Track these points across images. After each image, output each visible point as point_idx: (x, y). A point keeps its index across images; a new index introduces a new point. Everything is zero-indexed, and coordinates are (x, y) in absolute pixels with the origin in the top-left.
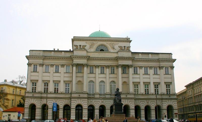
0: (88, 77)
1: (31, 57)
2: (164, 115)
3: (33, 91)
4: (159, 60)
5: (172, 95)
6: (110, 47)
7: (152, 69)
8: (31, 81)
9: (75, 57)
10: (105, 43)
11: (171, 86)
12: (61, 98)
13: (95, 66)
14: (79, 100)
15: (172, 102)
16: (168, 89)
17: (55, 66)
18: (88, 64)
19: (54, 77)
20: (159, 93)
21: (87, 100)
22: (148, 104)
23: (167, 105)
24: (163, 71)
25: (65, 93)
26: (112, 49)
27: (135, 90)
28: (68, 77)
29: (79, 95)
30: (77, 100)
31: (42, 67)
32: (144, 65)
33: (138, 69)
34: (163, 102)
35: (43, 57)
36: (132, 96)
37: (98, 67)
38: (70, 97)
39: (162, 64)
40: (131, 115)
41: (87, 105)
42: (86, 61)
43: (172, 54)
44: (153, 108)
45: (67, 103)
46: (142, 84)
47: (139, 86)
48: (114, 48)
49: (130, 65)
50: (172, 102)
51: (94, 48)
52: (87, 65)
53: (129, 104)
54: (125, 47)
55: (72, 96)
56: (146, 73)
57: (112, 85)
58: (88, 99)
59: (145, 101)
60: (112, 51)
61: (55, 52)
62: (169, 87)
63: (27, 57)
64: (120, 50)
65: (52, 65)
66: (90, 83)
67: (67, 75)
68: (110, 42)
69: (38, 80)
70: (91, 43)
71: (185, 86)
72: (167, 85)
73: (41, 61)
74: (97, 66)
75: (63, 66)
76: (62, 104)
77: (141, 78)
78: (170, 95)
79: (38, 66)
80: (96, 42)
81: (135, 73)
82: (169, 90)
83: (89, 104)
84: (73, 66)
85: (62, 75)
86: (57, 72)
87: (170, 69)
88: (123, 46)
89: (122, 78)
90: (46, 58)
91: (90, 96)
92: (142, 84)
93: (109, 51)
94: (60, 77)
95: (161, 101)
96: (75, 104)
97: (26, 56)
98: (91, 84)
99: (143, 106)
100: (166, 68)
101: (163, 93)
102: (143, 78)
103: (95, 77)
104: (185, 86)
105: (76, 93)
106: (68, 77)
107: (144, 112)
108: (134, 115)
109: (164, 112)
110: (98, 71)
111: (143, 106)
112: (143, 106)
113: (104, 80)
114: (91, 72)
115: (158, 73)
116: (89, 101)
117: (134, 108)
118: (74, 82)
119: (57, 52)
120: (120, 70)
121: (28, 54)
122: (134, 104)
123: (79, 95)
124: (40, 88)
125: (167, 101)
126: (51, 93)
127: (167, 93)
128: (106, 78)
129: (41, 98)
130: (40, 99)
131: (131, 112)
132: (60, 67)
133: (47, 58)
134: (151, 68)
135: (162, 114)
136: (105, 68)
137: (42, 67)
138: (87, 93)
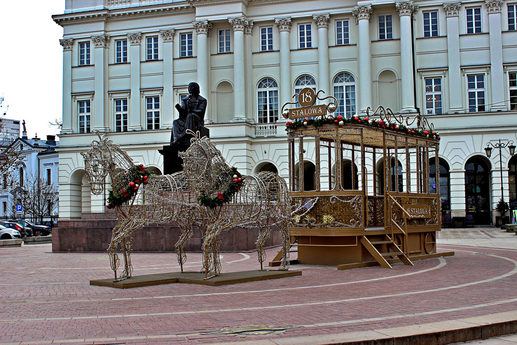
8: (74, 95)
13: (277, 21)
17: (144, 42)
18: (250, 19)
21: (244, 146)
31: (105, 47)
33: (441, 16)
35: (102, 13)
37: (290, 25)
42: (239, 7)
52: (248, 27)
63: (59, 20)
65: (136, 38)
66: (265, 87)
75: (169, 35)
77: (453, 50)
86: (153, 57)
97: (53, 16)
98: (268, 89)
103: (279, 65)
111: (457, 159)
114: (267, 48)
121: (61, 10)
124: (100, 116)
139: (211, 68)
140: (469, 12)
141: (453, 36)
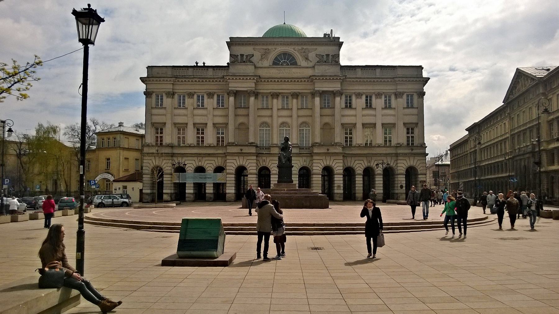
0: (259, 116)
1: (149, 81)
2: (399, 185)
3: (157, 144)
4: (396, 79)
5: (417, 146)
6: (301, 55)
7: (381, 98)
9: (233, 79)
10: (289, 49)
11: (416, 131)
12: (209, 155)
14: (241, 158)
15: (415, 161)
16: (410, 135)
19: (195, 117)
20: (394, 143)
22: (369, 164)
23: (405, 167)
24: (402, 101)
25: (216, 145)
26: (304, 61)
27: (346, 138)
28: (221, 116)
29: (241, 150)
30: (237, 158)
31: (173, 98)
32: (364, 91)
33: (354, 98)
34: (399, 161)
35: (172, 79)
36: (339, 150)
38: (224, 153)
39: (401, 88)
40: (336, 185)
41: (255, 168)
42: (253, 85)
43: (423, 68)
44: (379, 172)
45: (220, 164)
46: (359, 126)
47: (354, 132)
48: (307, 59)
49: (337, 91)
50: (415, 161)
51: (269, 58)
52: (256, 95)
53: (333, 165)
54: (328, 55)
55: (228, 151)
56: (369, 105)
57: (303, 130)
58: (257, 156)
59: (365, 159)
60: (303, 63)
61: (198, 68)
62: (412, 133)
63: (143, 80)
64: (318, 62)
65: (191, 95)
67: (217, 112)
68: (300, 48)
69: (165, 124)
70: (263, 49)
71: (467, 130)
72: (408, 129)
73: (169, 87)
74: (275, 95)
76: (211, 165)
78: (413, 148)
79: (165, 97)
80: (273, 47)
81: (349, 105)
82: (412, 137)
83: (259, 165)
84: (229, 94)
85: (210, 114)
87: (415, 97)
88: (324, 54)
89: (321, 116)
90: (178, 81)
91: (261, 151)
92: (359, 126)
93: (299, 64)
94: (206, 116)
95: (395, 158)
96: (234, 166)
97: (141, 78)
98: (265, 128)
99: (359, 167)
100: (408, 96)
101: (398, 144)
102: (363, 116)
103: (271, 116)
104: (467, 130)
105: (236, 145)
106: (221, 116)
107: (362, 179)
108: (342, 185)
109: (399, 179)
110: (276, 103)
112: (359, 167)
113: (288, 120)
115: (393, 105)
116: (261, 159)
117: (342, 171)
118: (231, 127)
119: (201, 69)
120: (317, 100)
122: (342, 165)
123: (241, 150)
125: (407, 159)
126: (190, 146)
127: (408, 144)
128: (291, 116)
129: (172, 156)
130: (170, 158)
131: (335, 179)
132: (206, 97)
133: (180, 80)
134: (379, 95)
135: (396, 182)
136: (290, 98)
137: (173, 98)
138: (254, 146)
139: (236, 115)
140: (367, 97)
141: (359, 109)
